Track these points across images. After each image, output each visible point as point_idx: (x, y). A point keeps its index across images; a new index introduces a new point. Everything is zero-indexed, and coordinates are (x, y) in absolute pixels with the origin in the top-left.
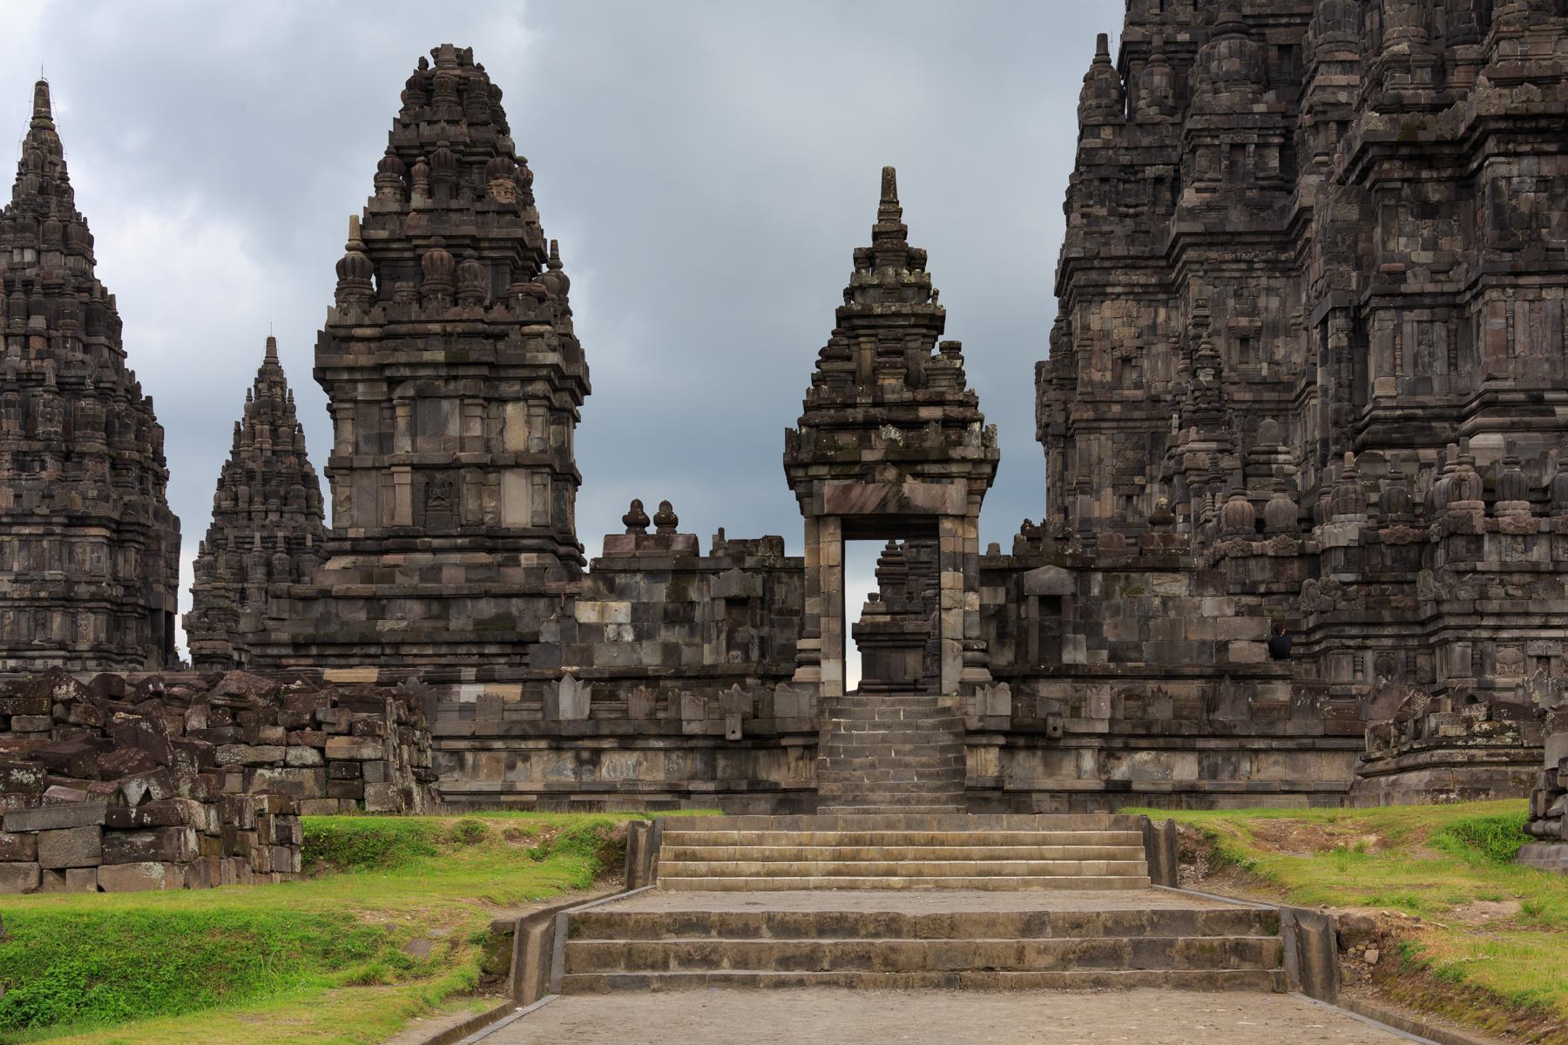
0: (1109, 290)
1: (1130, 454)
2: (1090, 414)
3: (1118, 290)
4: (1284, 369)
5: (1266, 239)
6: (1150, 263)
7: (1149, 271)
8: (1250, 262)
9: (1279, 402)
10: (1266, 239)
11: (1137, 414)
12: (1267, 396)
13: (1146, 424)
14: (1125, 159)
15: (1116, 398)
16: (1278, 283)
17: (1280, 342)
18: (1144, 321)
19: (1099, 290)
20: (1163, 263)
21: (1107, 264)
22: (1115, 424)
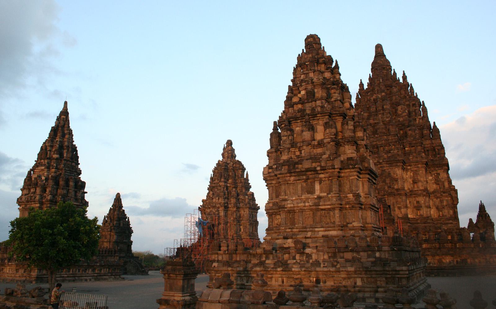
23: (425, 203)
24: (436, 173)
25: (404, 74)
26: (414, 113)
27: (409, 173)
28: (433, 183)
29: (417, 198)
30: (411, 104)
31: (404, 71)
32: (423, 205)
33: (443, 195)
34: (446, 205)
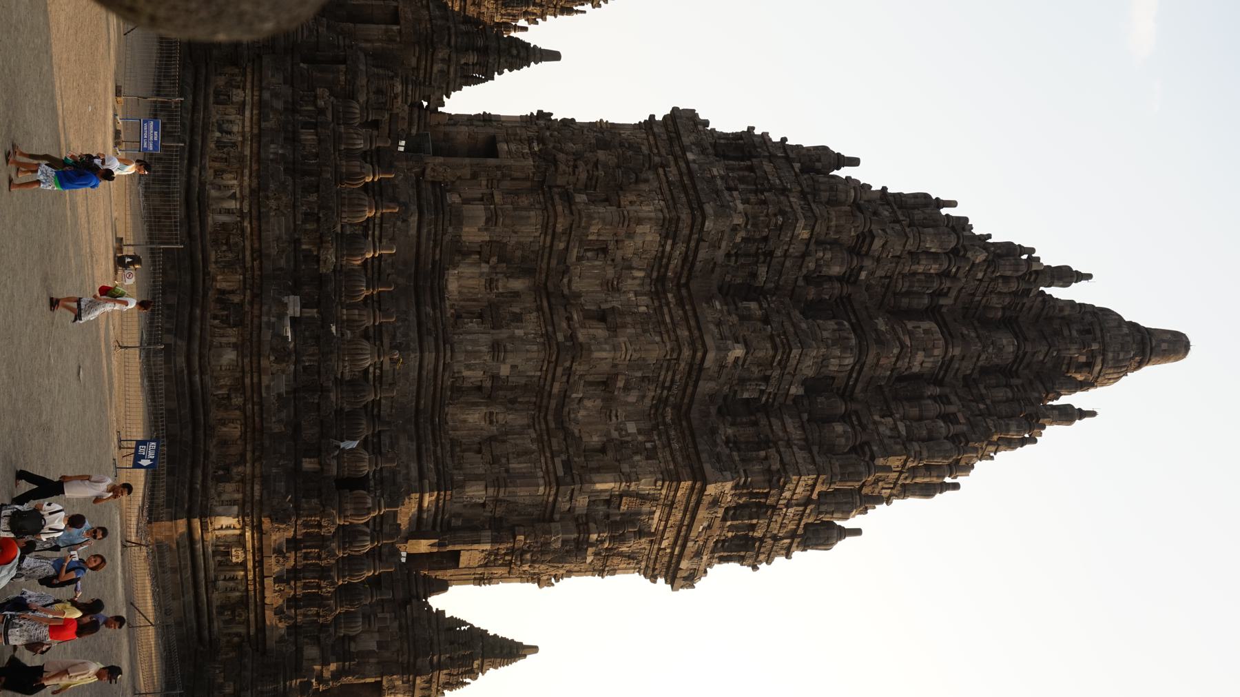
0: (670, 242)
1: (519, 253)
2: (559, 228)
3: (668, 248)
4: (576, 406)
5: (686, 401)
6: (685, 273)
7: (679, 270)
8: (670, 389)
9: (547, 408)
10: (686, 401)
11: (554, 262)
12: (553, 403)
13: (544, 266)
14: (779, 253)
15: (572, 244)
16: (648, 402)
17: (599, 403)
18: (636, 262)
19: (671, 234)
20: (683, 281)
21: (693, 244)
22: (548, 244)
23: (512, 338)
24: (655, 447)
25: (1082, 414)
26: (915, 412)
27: (645, 299)
28: (608, 434)
29: (538, 317)
30: (952, 409)
31: (1092, 414)
32: (503, 334)
33: (558, 461)
34: (507, 471)
